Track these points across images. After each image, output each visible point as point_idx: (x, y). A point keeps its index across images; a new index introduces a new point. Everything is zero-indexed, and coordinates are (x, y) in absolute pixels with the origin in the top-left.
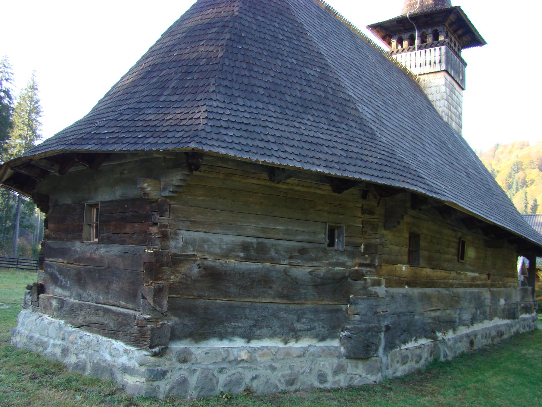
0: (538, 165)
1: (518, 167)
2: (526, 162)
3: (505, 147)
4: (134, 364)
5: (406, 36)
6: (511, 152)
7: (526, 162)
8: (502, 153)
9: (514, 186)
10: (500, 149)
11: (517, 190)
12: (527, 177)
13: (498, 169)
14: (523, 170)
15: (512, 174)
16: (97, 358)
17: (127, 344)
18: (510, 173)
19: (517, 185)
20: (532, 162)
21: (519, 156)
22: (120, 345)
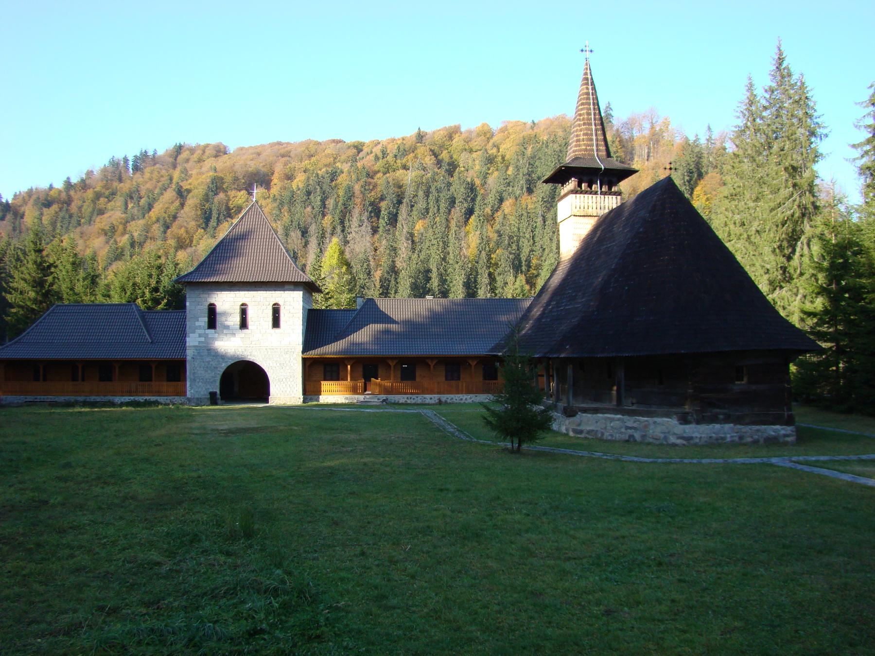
1: (217, 185)
2: (228, 178)
3: (192, 150)
4: (789, 432)
5: (585, 178)
6: (200, 161)
7: (228, 178)
8: (187, 161)
9: (215, 215)
10: (184, 155)
11: (219, 222)
13: (188, 187)
14: (225, 191)
15: (210, 196)
16: (765, 435)
17: (781, 425)
18: (207, 195)
19: (219, 214)
20: (236, 179)
22: (778, 427)
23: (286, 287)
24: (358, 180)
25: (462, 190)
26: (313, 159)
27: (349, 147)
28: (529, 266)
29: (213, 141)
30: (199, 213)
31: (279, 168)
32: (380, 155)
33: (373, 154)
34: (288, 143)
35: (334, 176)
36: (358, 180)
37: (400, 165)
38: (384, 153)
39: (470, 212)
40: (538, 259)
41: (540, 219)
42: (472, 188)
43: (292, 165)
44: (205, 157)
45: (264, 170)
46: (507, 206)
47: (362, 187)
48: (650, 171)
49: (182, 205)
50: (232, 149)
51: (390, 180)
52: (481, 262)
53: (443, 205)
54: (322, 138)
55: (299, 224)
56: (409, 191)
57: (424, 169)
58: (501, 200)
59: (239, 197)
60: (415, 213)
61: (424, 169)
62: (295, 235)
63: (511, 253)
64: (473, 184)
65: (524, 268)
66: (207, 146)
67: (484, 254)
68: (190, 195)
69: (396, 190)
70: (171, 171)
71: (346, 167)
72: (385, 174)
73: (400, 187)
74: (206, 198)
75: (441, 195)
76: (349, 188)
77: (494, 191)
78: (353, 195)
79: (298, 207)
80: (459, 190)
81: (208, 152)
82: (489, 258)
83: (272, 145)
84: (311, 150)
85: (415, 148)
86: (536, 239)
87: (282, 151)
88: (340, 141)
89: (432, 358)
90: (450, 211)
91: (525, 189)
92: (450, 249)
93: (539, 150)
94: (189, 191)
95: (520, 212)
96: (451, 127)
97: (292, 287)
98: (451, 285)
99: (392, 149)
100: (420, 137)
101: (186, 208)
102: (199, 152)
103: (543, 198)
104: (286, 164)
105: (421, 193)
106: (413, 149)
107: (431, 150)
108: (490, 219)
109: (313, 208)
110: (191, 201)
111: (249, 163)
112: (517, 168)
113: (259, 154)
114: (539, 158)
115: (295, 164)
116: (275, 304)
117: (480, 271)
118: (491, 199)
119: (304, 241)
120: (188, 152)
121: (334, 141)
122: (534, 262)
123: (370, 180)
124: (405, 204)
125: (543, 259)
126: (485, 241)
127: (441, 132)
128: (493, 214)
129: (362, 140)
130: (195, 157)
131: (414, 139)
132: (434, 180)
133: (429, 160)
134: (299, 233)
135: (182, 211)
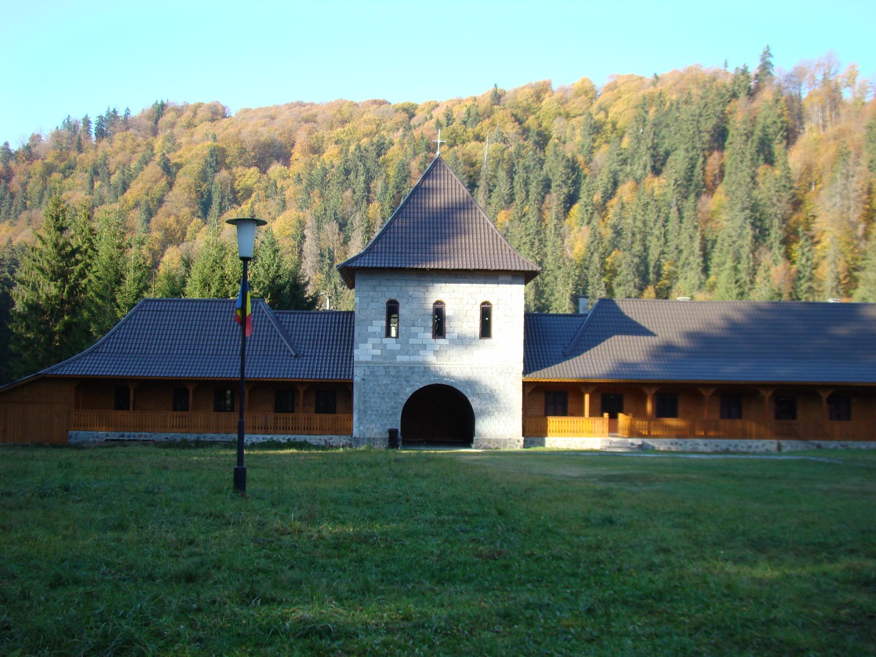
0: (254, 157)
1: (218, 159)
2: (233, 151)
3: (179, 111)
6: (190, 125)
7: (233, 151)
8: (173, 125)
9: (216, 199)
10: (168, 117)
12: (237, 182)
13: (178, 161)
14: (228, 167)
15: (209, 174)
21: (218, 138)
23: (501, 278)
24: (415, 154)
25: (561, 169)
26: (348, 126)
27: (397, 111)
28: (658, 275)
29: (208, 100)
30: (194, 196)
31: (301, 138)
32: (443, 120)
33: (434, 120)
34: (312, 104)
35: (381, 148)
36: (415, 154)
37: (471, 135)
38: (449, 119)
39: (571, 200)
40: (670, 264)
41: (674, 209)
42: (573, 167)
43: (320, 134)
44: (196, 121)
45: (282, 140)
46: (625, 190)
47: (421, 164)
48: (831, 142)
49: (171, 185)
50: (233, 110)
51: (459, 154)
52: (592, 267)
53: (534, 189)
54: (360, 97)
55: (335, 214)
56: (486, 170)
57: (505, 141)
58: (615, 184)
59: (249, 176)
60: (494, 200)
61: (505, 141)
62: (331, 228)
63: (635, 256)
64: (574, 162)
65: (652, 277)
66: (199, 105)
67: (596, 258)
68: (181, 171)
69: (467, 168)
70: (150, 138)
71: (397, 137)
72: (451, 146)
73: (473, 165)
74: (204, 176)
75: (531, 176)
76: (403, 165)
77: (605, 171)
78: (409, 175)
79: (333, 191)
80: (557, 171)
81: (201, 114)
82: (603, 264)
83: (291, 106)
84: (344, 115)
85: (492, 112)
86: (669, 237)
87: (305, 115)
88: (384, 103)
89: (707, 385)
90: (543, 198)
91: (648, 168)
92: (549, 250)
93: (667, 114)
94: (179, 166)
95: (645, 199)
96: (538, 84)
97: (509, 278)
98: (552, 298)
99: (459, 113)
100: (497, 97)
101: (176, 190)
102: (189, 113)
103: (676, 181)
104: (310, 133)
105: (502, 174)
106: (489, 113)
107: (513, 115)
108: (602, 208)
109: (354, 192)
110: (184, 180)
111: (261, 129)
112: (638, 139)
113: (273, 118)
114: (667, 126)
115: (323, 132)
116: (484, 303)
117: (590, 280)
118: (602, 180)
119: (342, 236)
120: (173, 114)
121: (375, 102)
122: (666, 268)
123: (431, 155)
124: (481, 188)
125: (680, 263)
126: (597, 238)
127: (527, 90)
128: (605, 202)
129: (413, 100)
130: (184, 120)
131: (489, 99)
132: (519, 155)
133: (511, 129)
134: (336, 227)
135: (170, 194)
